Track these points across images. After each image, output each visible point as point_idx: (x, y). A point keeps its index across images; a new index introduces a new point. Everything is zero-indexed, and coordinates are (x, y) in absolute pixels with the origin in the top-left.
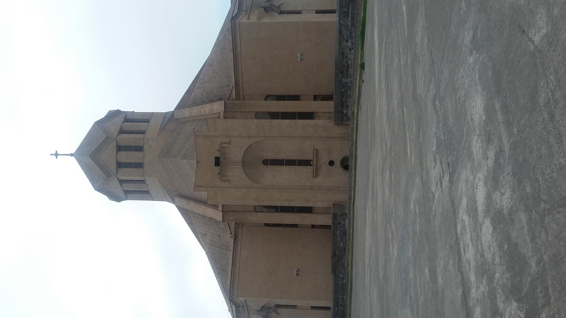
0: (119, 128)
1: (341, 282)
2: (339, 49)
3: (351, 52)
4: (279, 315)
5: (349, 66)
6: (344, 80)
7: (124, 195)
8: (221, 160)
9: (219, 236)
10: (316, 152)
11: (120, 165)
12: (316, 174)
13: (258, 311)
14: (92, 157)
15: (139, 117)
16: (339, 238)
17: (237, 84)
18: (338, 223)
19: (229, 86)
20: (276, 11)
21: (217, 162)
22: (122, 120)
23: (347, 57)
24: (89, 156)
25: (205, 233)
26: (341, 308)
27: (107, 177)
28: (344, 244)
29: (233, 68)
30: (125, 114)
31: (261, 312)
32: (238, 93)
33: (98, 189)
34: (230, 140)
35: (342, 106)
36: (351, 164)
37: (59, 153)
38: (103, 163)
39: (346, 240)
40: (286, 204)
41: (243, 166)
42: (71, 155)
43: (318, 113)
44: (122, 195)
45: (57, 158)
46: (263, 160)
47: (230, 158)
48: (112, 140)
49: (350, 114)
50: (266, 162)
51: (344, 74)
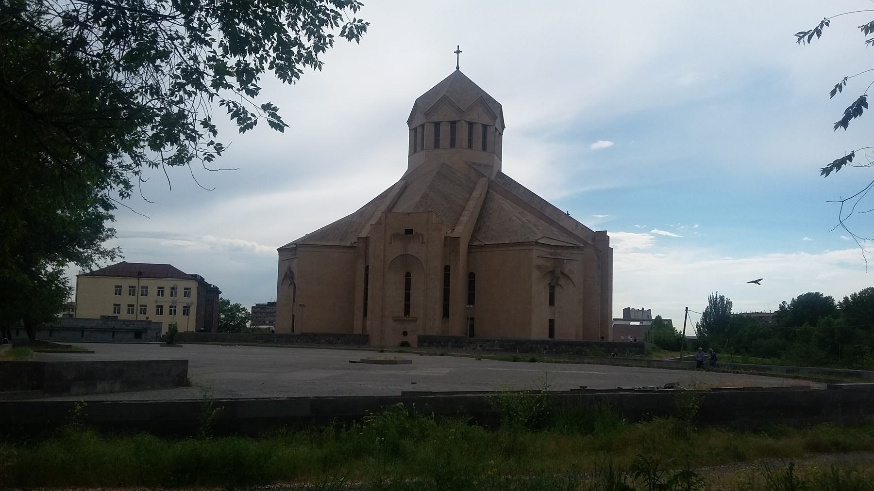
1: (294, 340)
4: (289, 286)
6: (450, 344)
12: (396, 320)
13: (290, 268)
16: (327, 339)
17: (485, 246)
21: (409, 232)
22: (484, 123)
27: (425, 114)
28: (323, 343)
29: (496, 243)
30: (492, 124)
32: (477, 247)
36: (402, 349)
40: (369, 294)
41: (403, 255)
42: (458, 68)
43: (448, 321)
44: (413, 126)
45: (455, 52)
50: (408, 275)
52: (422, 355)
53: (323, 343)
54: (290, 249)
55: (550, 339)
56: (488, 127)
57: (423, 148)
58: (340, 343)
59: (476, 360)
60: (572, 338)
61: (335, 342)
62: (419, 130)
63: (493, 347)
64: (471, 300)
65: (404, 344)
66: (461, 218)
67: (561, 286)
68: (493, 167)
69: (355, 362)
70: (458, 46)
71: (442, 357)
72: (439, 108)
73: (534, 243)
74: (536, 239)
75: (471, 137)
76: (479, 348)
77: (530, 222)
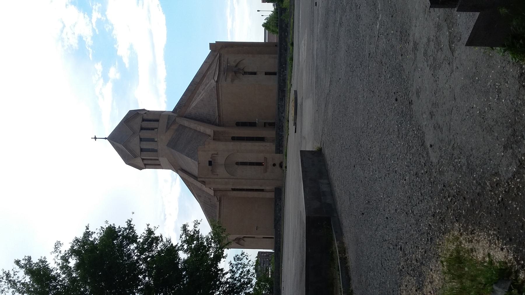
7: (144, 166)
8: (213, 163)
10: (266, 159)
11: (142, 150)
13: (233, 240)
14: (125, 145)
17: (219, 116)
20: (241, 73)
21: (210, 163)
23: (282, 122)
29: (217, 108)
30: (142, 115)
34: (218, 153)
40: (250, 188)
41: (225, 167)
42: (106, 138)
44: (144, 166)
45: (96, 140)
50: (237, 163)
52: (289, 134)
53: (280, 215)
55: (277, 75)
56: (144, 118)
57: (158, 159)
58: (281, 203)
59: (292, 87)
60: (277, 61)
61: (279, 207)
62: (146, 162)
64: (252, 125)
65: (281, 166)
66: (202, 131)
67: (245, 67)
68: (169, 115)
69: (296, 128)
71: (290, 122)
72: (131, 149)
73: (217, 83)
74: (214, 82)
75: (150, 129)
76: (283, 115)
77: (204, 88)
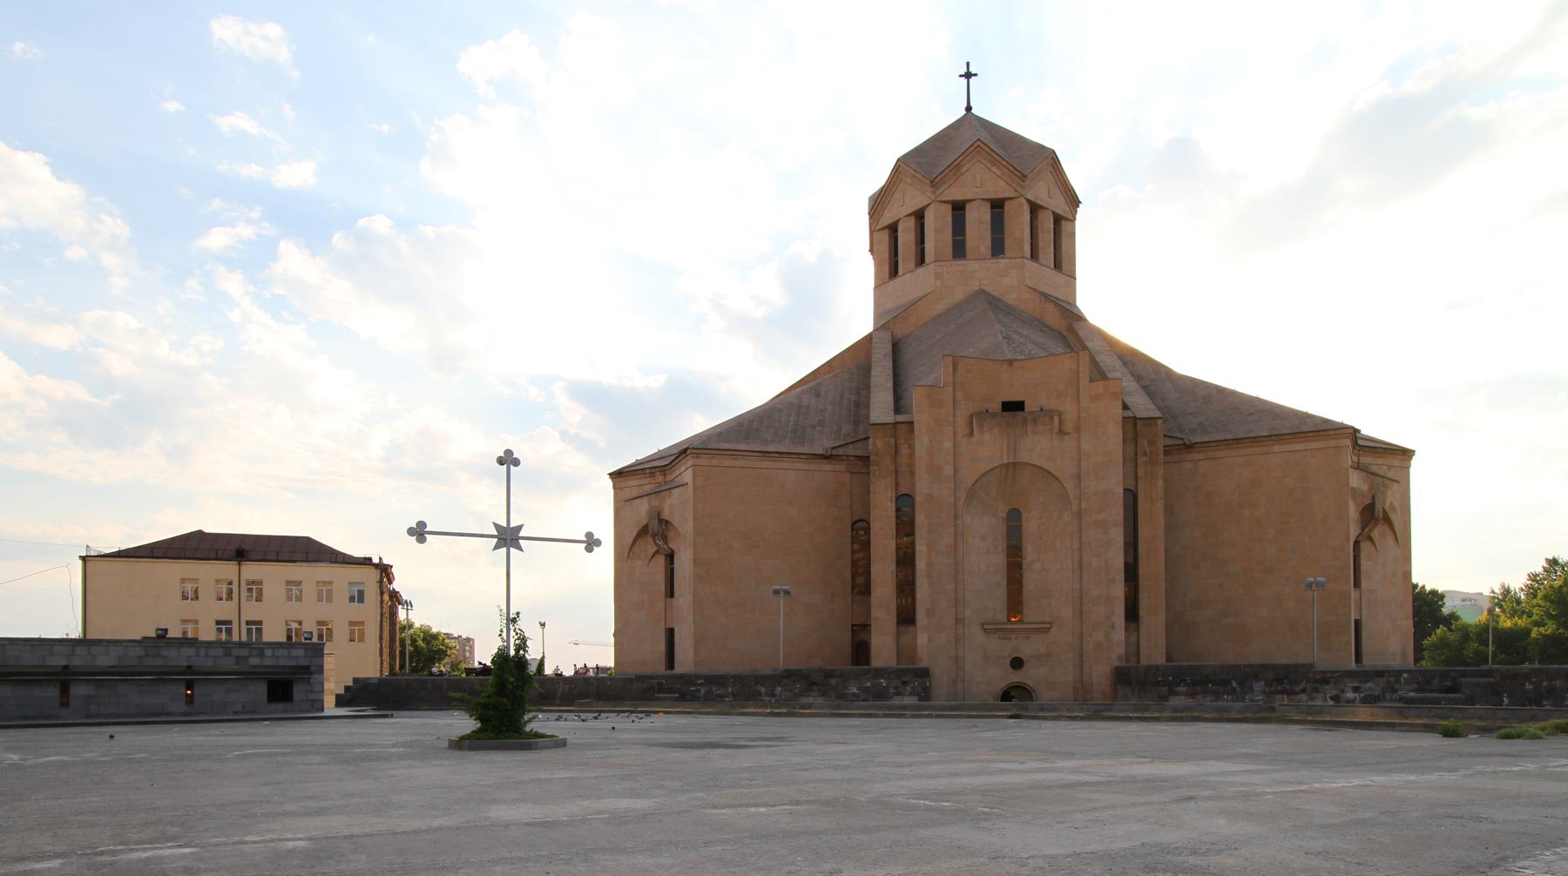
0: (1042, 204)
1: (763, 690)
2: (1337, 672)
3: (1329, 700)
5: (1293, 697)
8: (1021, 413)
9: (822, 423)
15: (1064, 247)
16: (869, 684)
18: (905, 680)
19: (1181, 431)
21: (1013, 407)
22: (1058, 211)
23: (1316, 690)
24: (978, 140)
25: (822, 393)
26: (703, 692)
27: (932, 182)
28: (854, 694)
29: (1229, 437)
30: (1070, 217)
31: (657, 521)
33: (899, 166)
34: (1068, 434)
35: (1194, 683)
37: (972, 80)
38: (963, 170)
39: (864, 700)
41: (1007, 465)
42: (969, 108)
44: (887, 219)
46: (1019, 511)
47: (1026, 433)
48: (1019, 189)
49: (1175, 701)
50: (1014, 520)
51: (1275, 684)
54: (648, 471)
63: (1397, 691)
70: (968, 64)
76: (1350, 695)
